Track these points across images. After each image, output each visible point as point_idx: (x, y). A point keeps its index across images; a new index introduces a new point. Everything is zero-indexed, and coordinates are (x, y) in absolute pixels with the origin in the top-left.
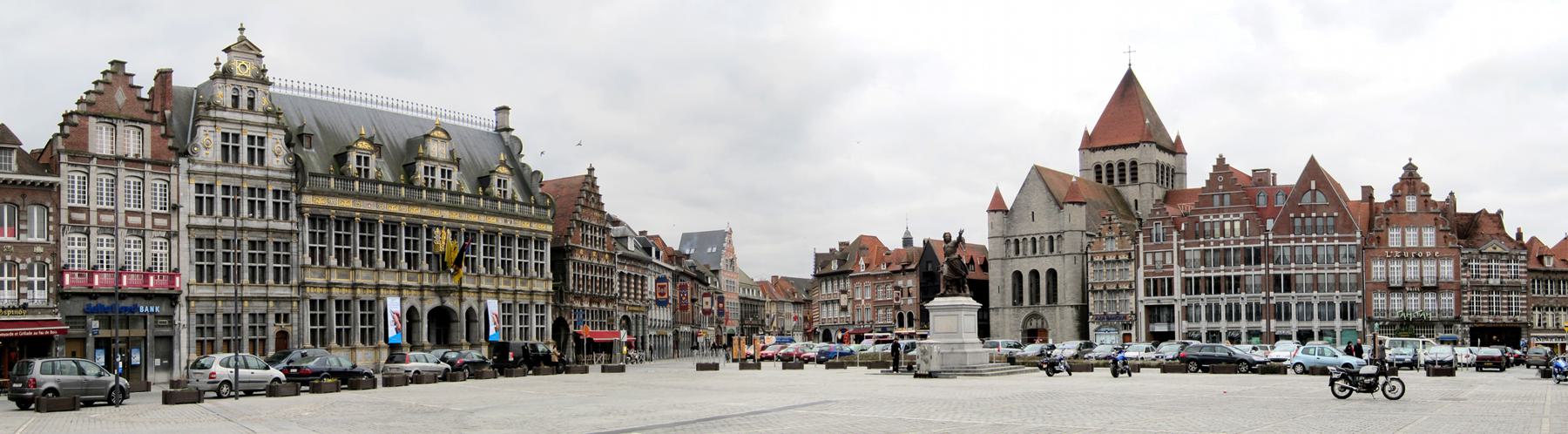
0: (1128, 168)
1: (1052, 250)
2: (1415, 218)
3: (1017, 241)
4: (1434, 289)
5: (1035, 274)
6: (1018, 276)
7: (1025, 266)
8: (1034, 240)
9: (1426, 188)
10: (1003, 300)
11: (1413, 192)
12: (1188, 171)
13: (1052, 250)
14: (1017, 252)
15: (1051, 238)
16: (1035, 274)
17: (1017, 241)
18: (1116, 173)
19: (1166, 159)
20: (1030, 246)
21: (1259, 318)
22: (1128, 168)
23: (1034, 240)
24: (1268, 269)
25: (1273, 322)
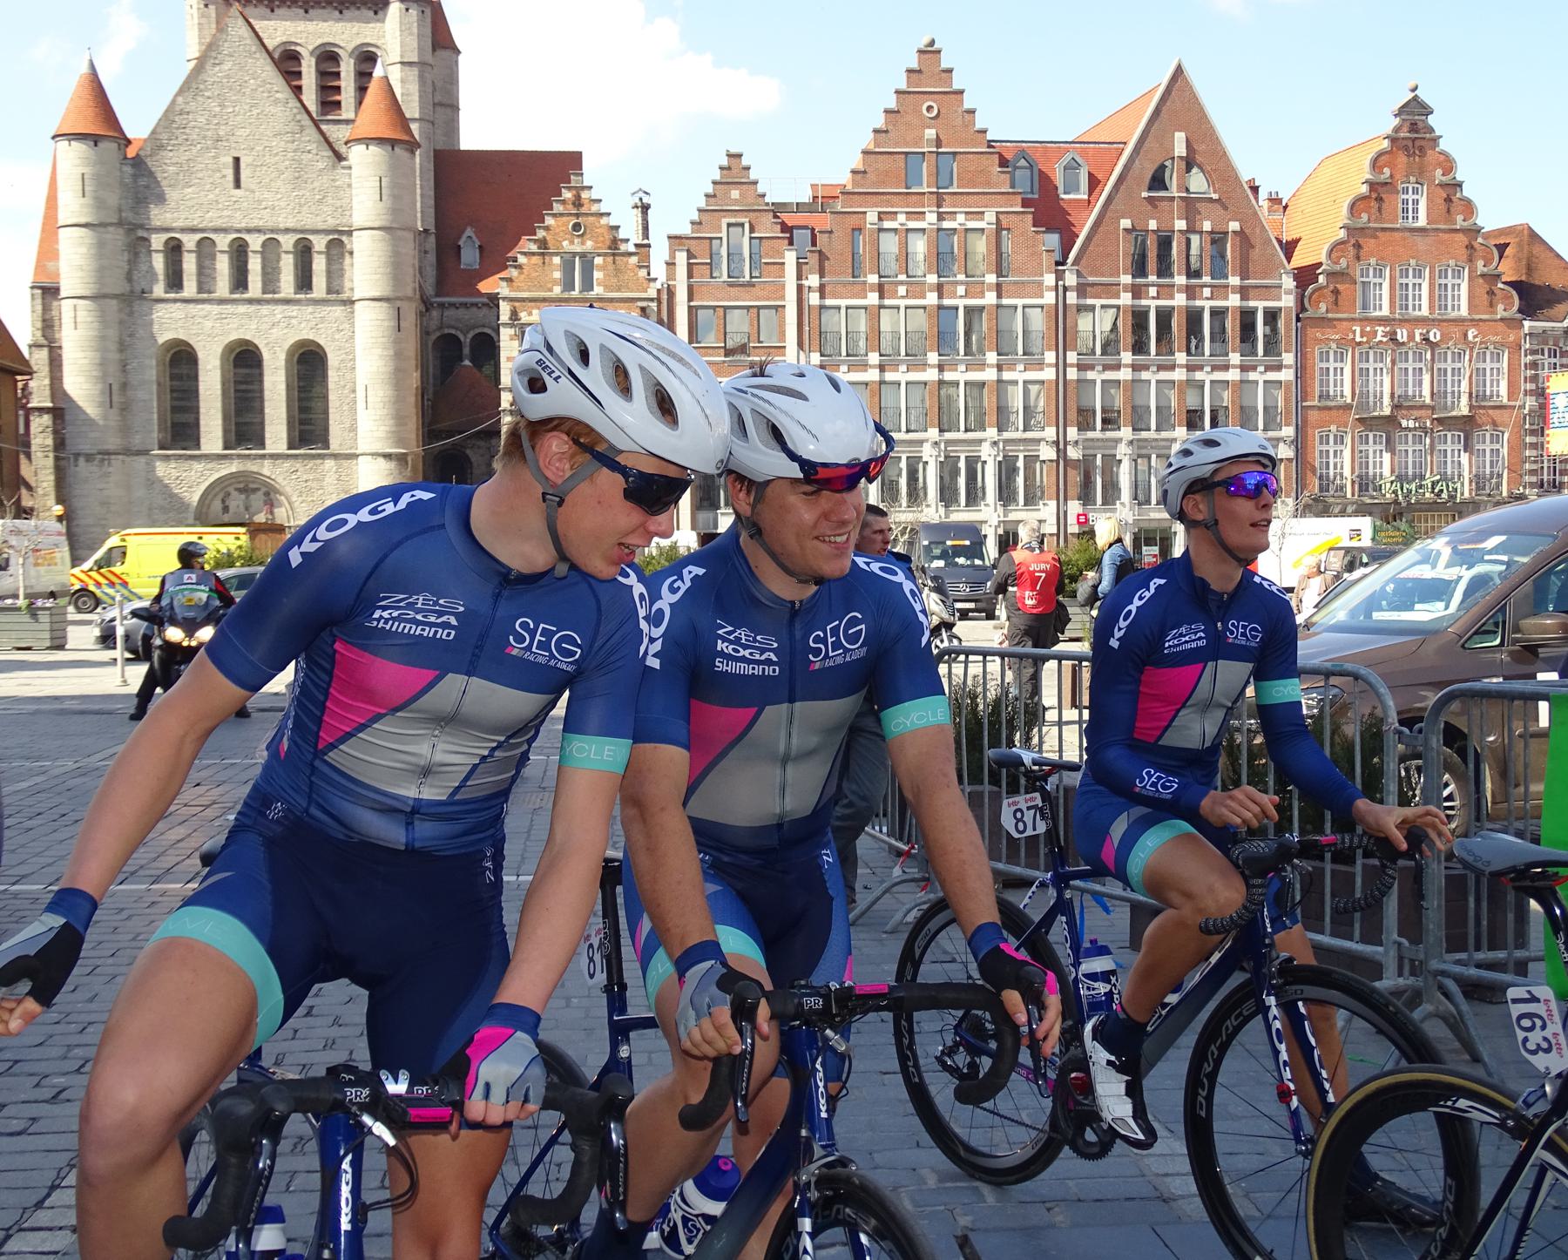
0: (347, 69)
1: (304, 281)
2: (1421, 243)
3: (174, 250)
4: (1467, 427)
5: (244, 359)
6: (182, 359)
7: (208, 328)
8: (239, 252)
9: (1448, 164)
10: (125, 430)
11: (1421, 174)
12: (461, 106)
13: (304, 281)
14: (175, 280)
15: (304, 253)
16: (244, 359)
17: (174, 250)
18: (309, 80)
19: (429, 58)
20: (223, 265)
21: (1030, 500)
22: (347, 69)
23: (239, 252)
24: (1061, 365)
25: (1074, 507)
